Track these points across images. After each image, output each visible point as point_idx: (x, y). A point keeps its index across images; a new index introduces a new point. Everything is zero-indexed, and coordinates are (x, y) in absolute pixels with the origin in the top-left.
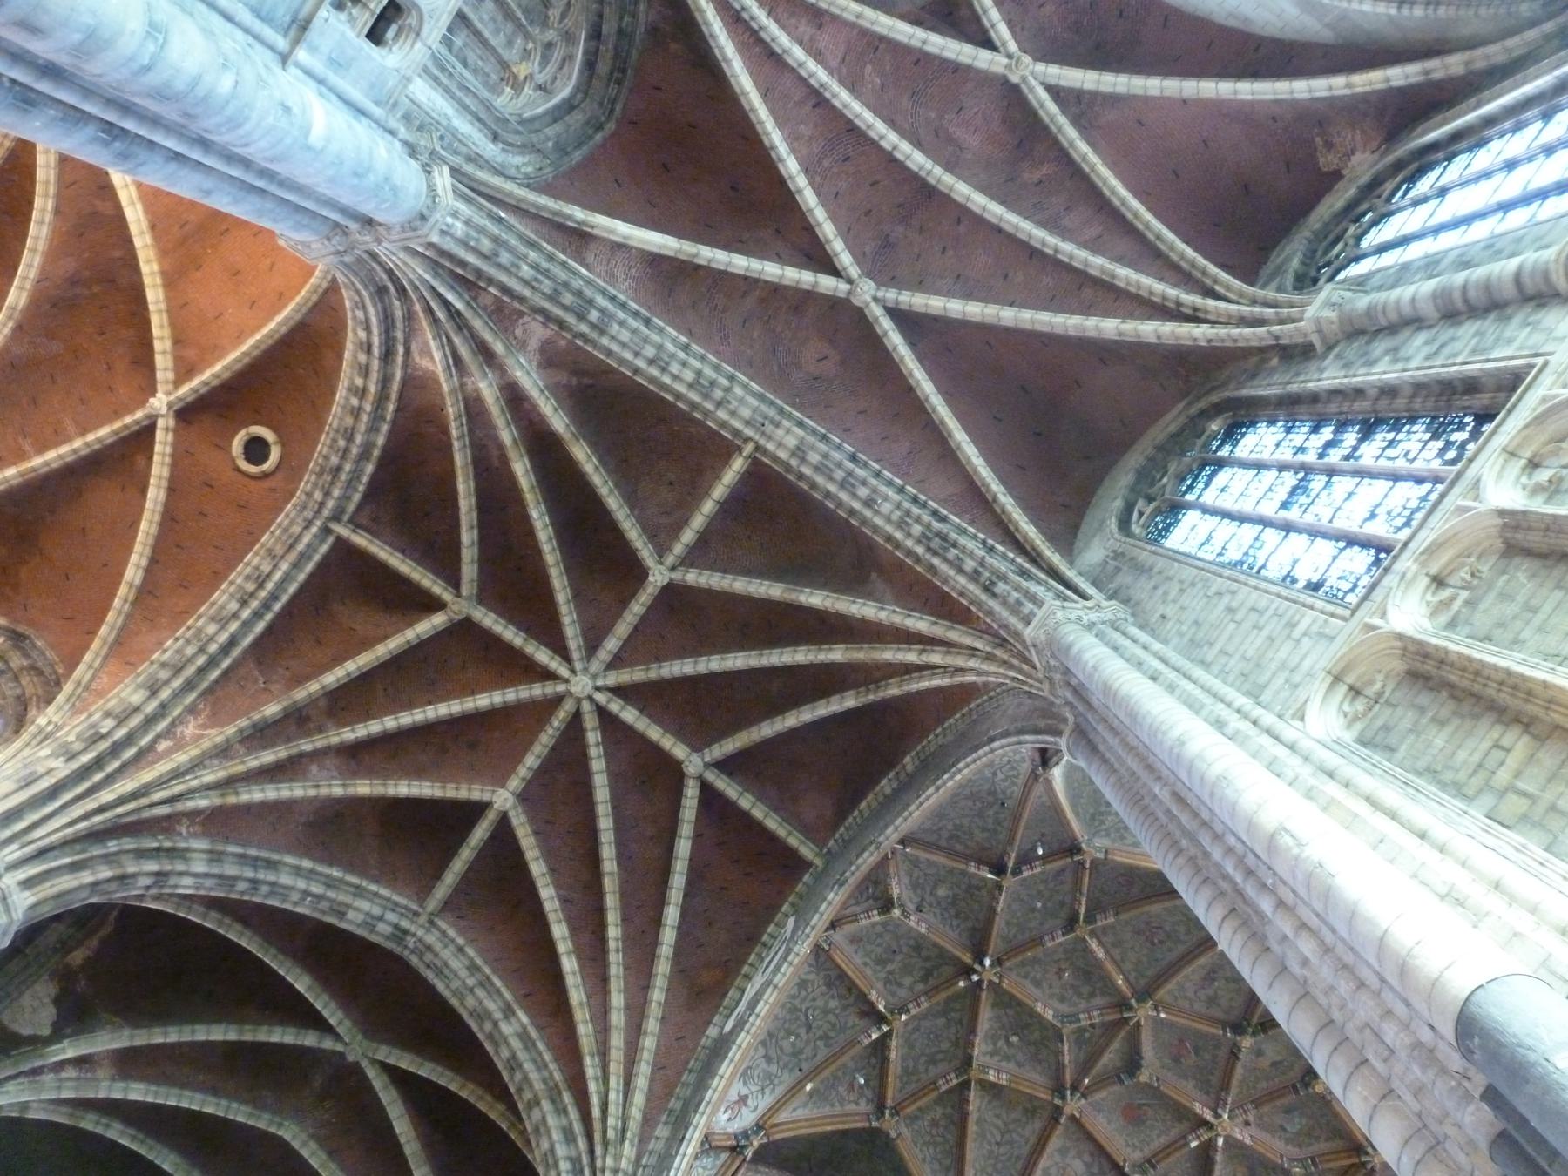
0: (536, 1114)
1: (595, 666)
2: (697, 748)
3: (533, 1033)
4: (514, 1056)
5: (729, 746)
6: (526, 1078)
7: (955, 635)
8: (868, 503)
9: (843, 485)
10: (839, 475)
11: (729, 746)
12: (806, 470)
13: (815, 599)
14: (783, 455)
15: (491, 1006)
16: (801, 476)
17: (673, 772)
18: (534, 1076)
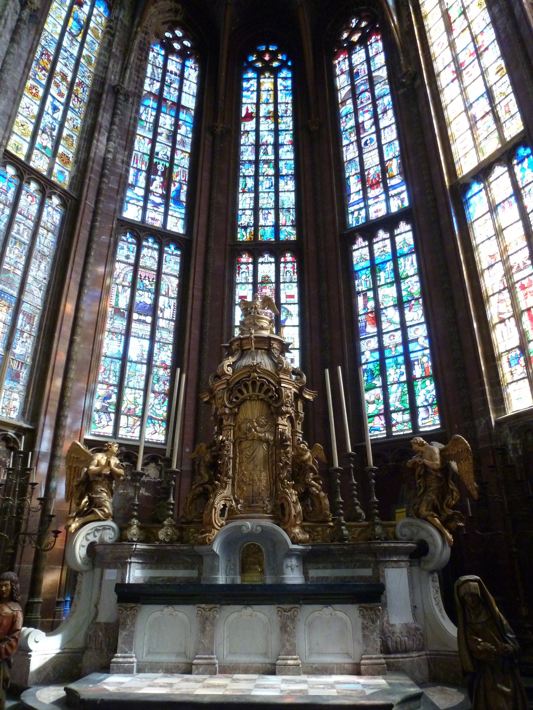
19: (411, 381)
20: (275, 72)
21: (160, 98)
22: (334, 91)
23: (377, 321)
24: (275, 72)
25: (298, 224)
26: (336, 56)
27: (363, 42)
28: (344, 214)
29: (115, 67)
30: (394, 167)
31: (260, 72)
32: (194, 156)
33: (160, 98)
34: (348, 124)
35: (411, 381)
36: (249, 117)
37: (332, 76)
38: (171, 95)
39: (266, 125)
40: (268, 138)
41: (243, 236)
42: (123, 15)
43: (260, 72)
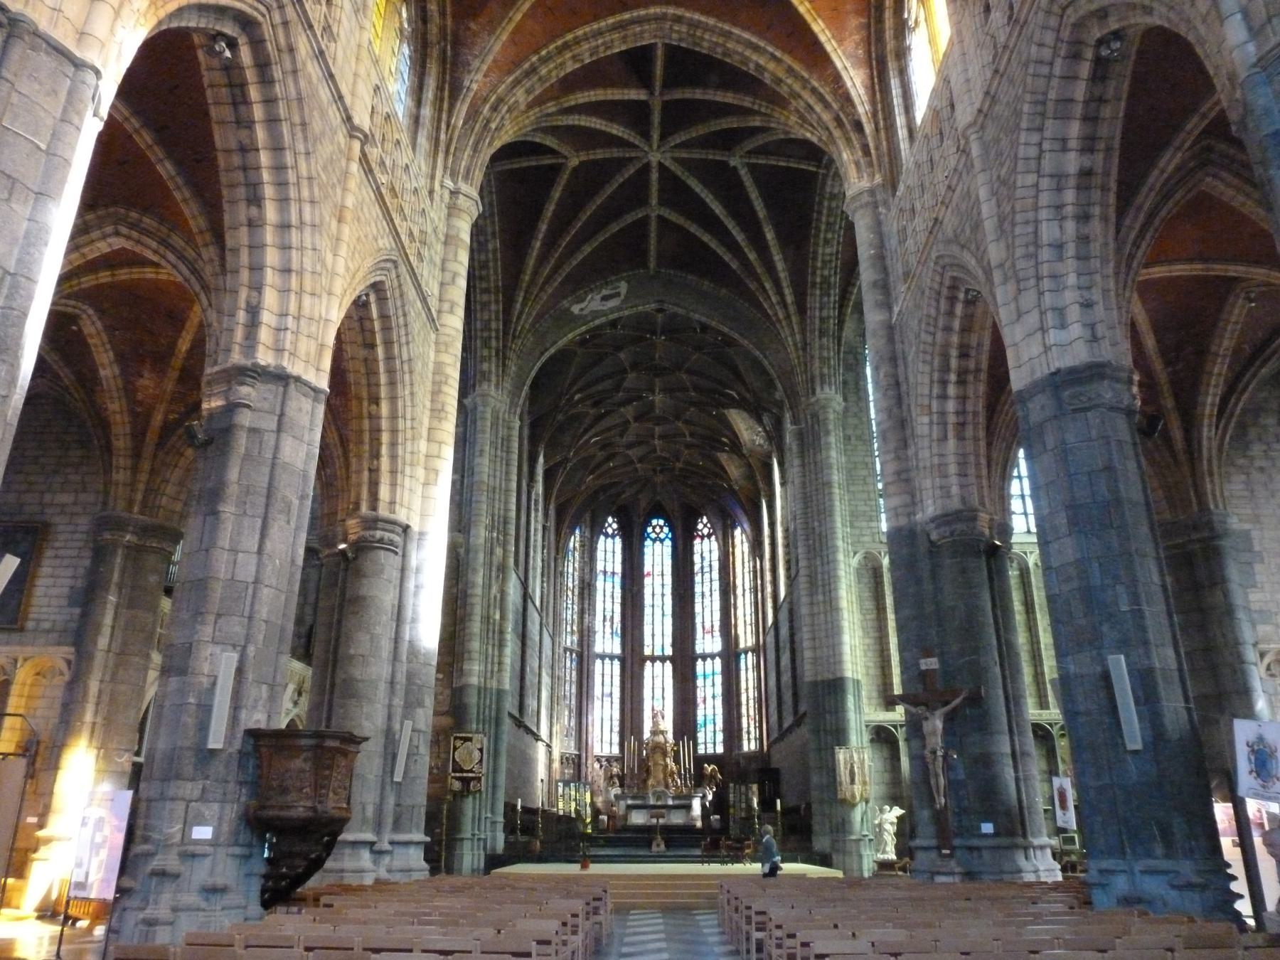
0: (485, 298)
1: (668, 155)
2: (662, 202)
3: (499, 255)
4: (487, 261)
5: (673, 217)
6: (488, 275)
7: (794, 319)
8: (827, 242)
9: (828, 224)
10: (832, 220)
11: (673, 217)
12: (826, 203)
13: (770, 235)
14: (828, 190)
15: (489, 230)
16: (821, 203)
17: (643, 201)
18: (492, 278)
19: (715, 732)
20: (662, 541)
21: (605, 573)
22: (692, 564)
23: (704, 701)
24: (662, 541)
25: (673, 645)
26: (694, 538)
27: (709, 536)
28: (693, 644)
29: (587, 570)
30: (717, 627)
31: (654, 540)
32: (623, 605)
33: (605, 573)
34: (698, 589)
35: (715, 732)
36: (648, 574)
37: (692, 553)
38: (609, 569)
39: (658, 580)
40: (658, 590)
41: (647, 652)
42: (588, 534)
43: (654, 540)
